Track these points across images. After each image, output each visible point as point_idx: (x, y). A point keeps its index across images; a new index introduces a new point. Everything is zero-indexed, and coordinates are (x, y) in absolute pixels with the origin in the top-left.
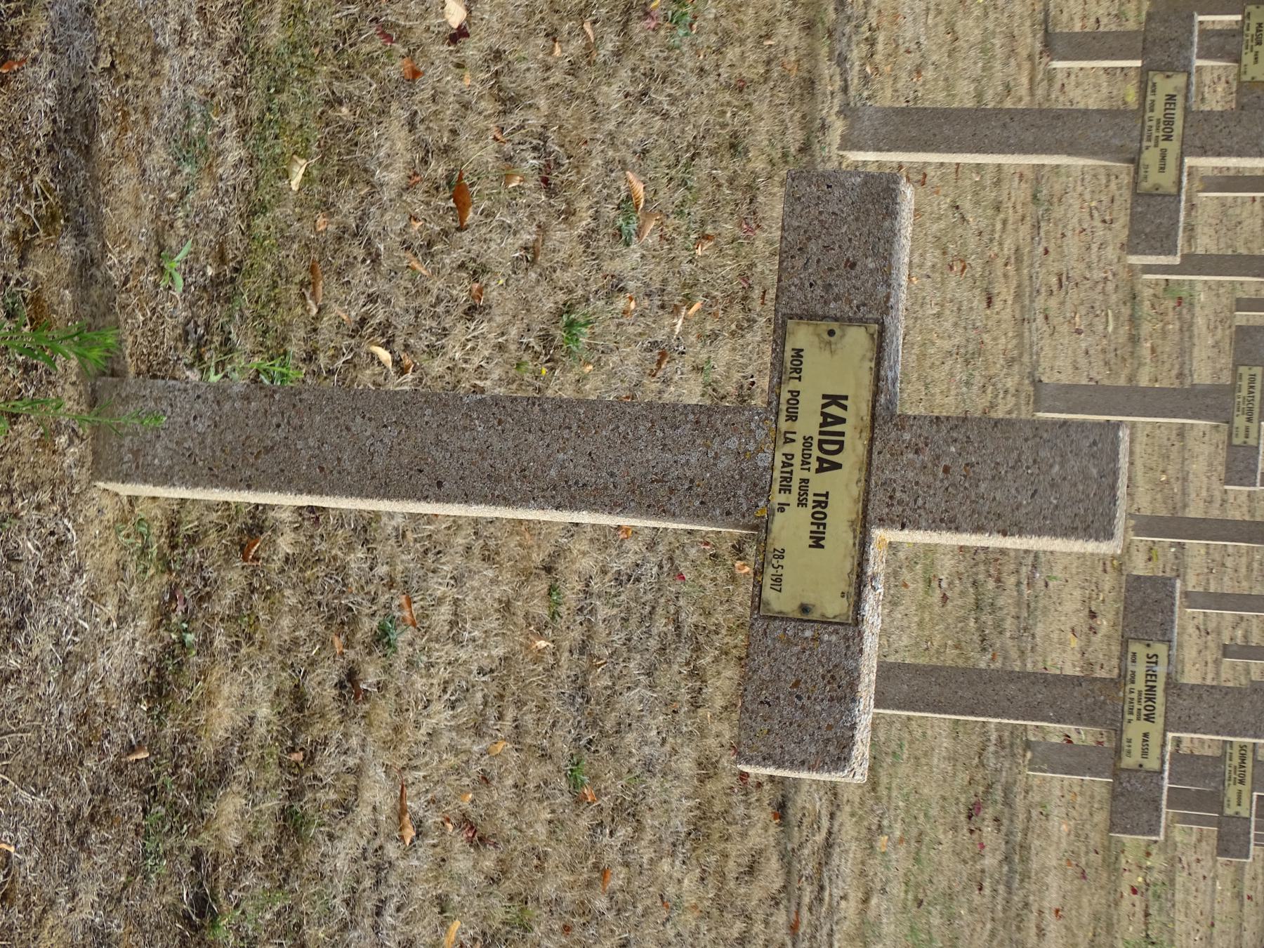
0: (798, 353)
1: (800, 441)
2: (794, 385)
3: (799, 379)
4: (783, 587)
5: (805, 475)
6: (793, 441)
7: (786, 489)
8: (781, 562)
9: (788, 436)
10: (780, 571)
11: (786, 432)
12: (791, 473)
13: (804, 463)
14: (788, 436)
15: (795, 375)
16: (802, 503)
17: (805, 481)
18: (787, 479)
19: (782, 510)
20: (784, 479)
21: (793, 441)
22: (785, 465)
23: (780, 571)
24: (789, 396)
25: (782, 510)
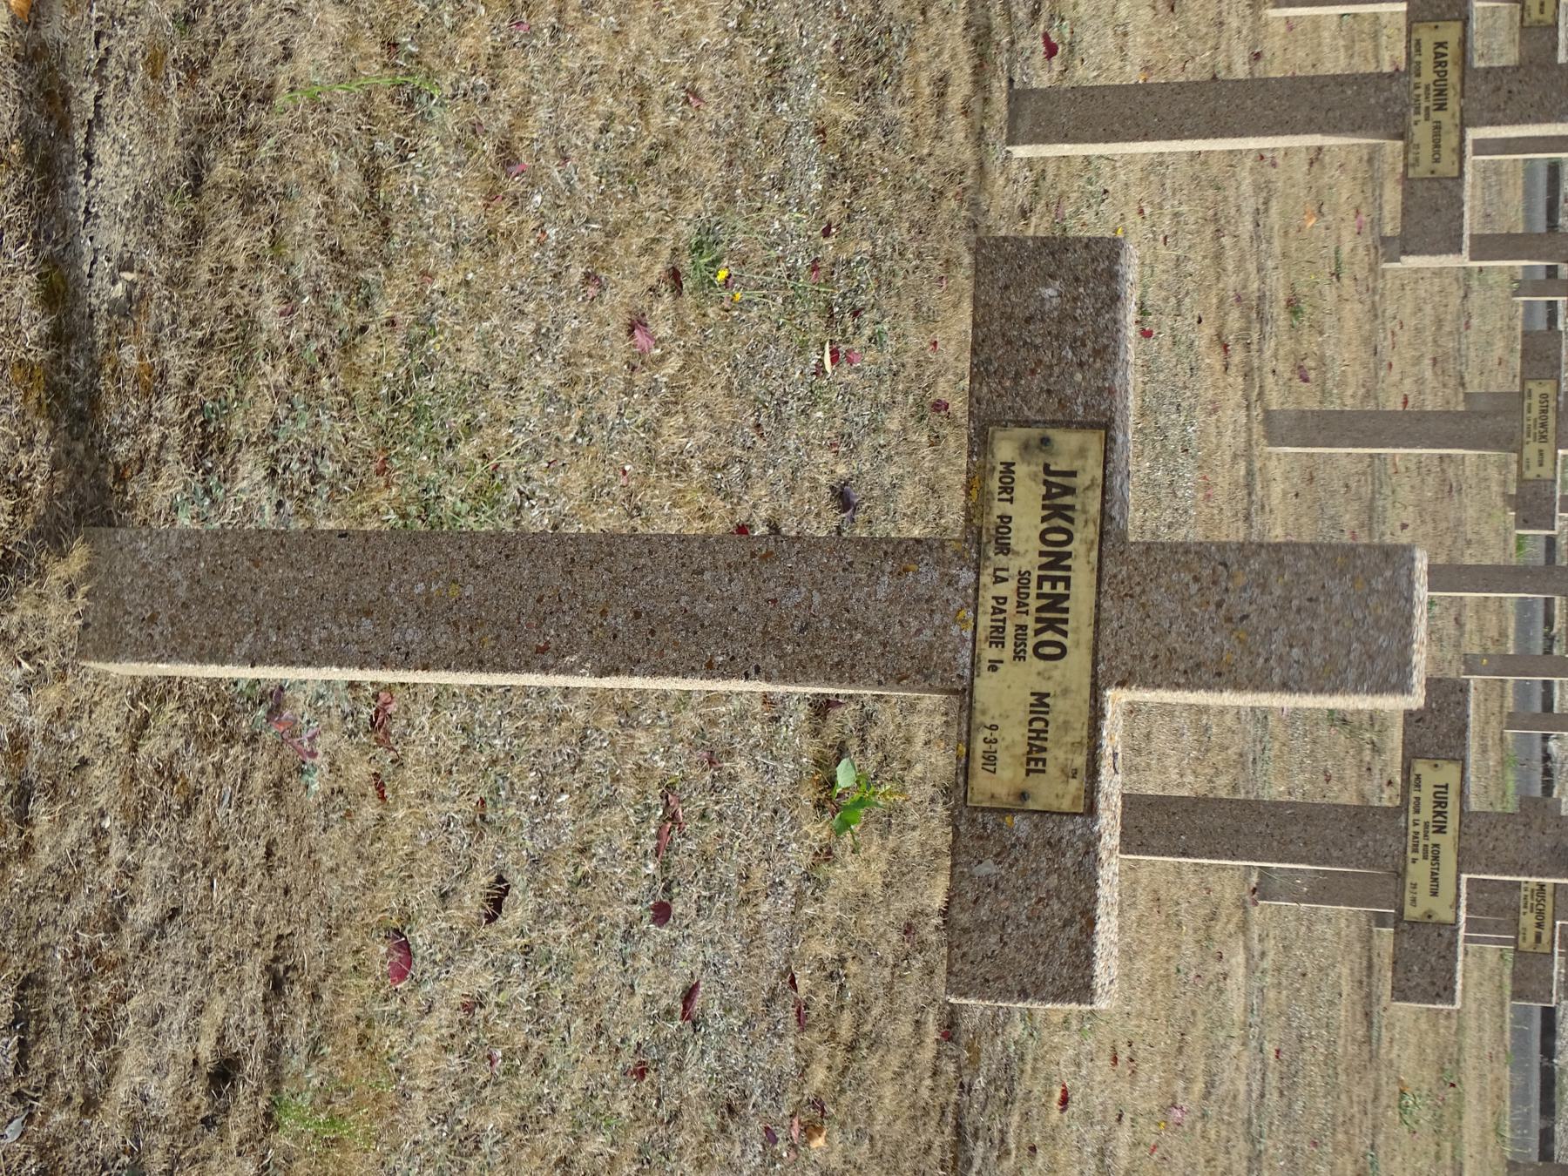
2: (1006, 508)
4: (998, 767)
6: (1005, 580)
8: (996, 734)
9: (998, 573)
12: (1004, 620)
14: (999, 573)
15: (1005, 496)
16: (1019, 656)
17: (1023, 628)
19: (993, 668)
22: (996, 611)
25: (993, 668)
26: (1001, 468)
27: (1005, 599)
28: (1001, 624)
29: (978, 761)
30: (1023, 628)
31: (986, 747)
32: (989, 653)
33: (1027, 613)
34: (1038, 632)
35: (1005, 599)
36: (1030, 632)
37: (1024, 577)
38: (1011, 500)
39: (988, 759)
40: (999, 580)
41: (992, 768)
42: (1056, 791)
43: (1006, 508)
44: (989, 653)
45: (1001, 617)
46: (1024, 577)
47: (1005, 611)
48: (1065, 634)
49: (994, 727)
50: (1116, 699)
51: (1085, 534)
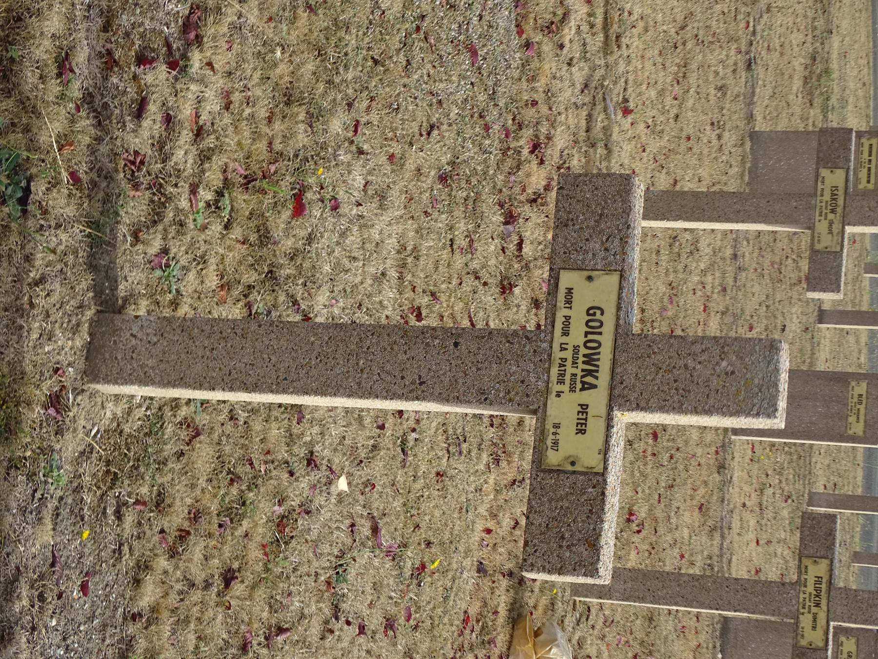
0: (570, 291)
2: (567, 312)
3: (571, 308)
5: (574, 371)
6: (566, 349)
7: (561, 382)
8: (559, 431)
12: (565, 370)
13: (573, 363)
15: (567, 305)
16: (572, 390)
17: (575, 375)
18: (562, 375)
19: (558, 395)
20: (560, 375)
21: (566, 349)
22: (561, 365)
24: (564, 319)
25: (558, 395)
29: (549, 443)
31: (553, 437)
32: (557, 388)
33: (577, 367)
34: (582, 377)
38: (571, 308)
40: (563, 349)
42: (590, 460)
43: (567, 312)
44: (557, 388)
45: (563, 368)
46: (576, 349)
49: (557, 426)
51: (608, 329)
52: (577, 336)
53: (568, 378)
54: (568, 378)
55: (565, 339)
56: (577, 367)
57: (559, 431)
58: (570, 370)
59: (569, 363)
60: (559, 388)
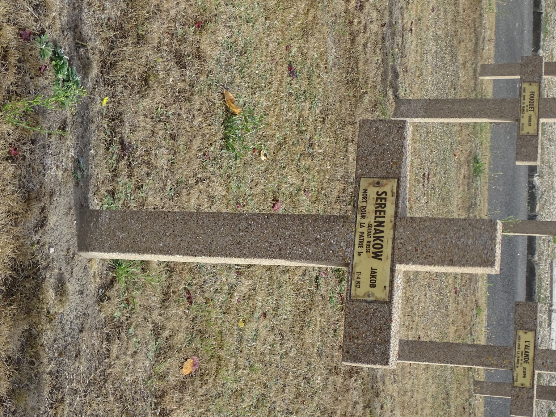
1: (366, 225)
3: (366, 201)
6: (364, 226)
9: (362, 224)
10: (359, 280)
11: (361, 223)
12: (363, 239)
13: (368, 235)
14: (362, 224)
15: (364, 200)
16: (368, 251)
20: (360, 242)
21: (364, 226)
22: (360, 236)
23: (359, 280)
25: (359, 254)
26: (363, 191)
27: (364, 232)
28: (362, 241)
30: (369, 242)
33: (370, 237)
35: (364, 232)
36: (372, 243)
37: (370, 226)
39: (357, 283)
41: (359, 286)
42: (379, 293)
45: (362, 238)
47: (363, 236)
48: (382, 241)
49: (360, 273)
50: (400, 268)
52: (370, 218)
53: (365, 243)
54: (365, 243)
55: (363, 221)
56: (370, 237)
57: (360, 276)
58: (366, 239)
59: (365, 235)
60: (360, 250)
